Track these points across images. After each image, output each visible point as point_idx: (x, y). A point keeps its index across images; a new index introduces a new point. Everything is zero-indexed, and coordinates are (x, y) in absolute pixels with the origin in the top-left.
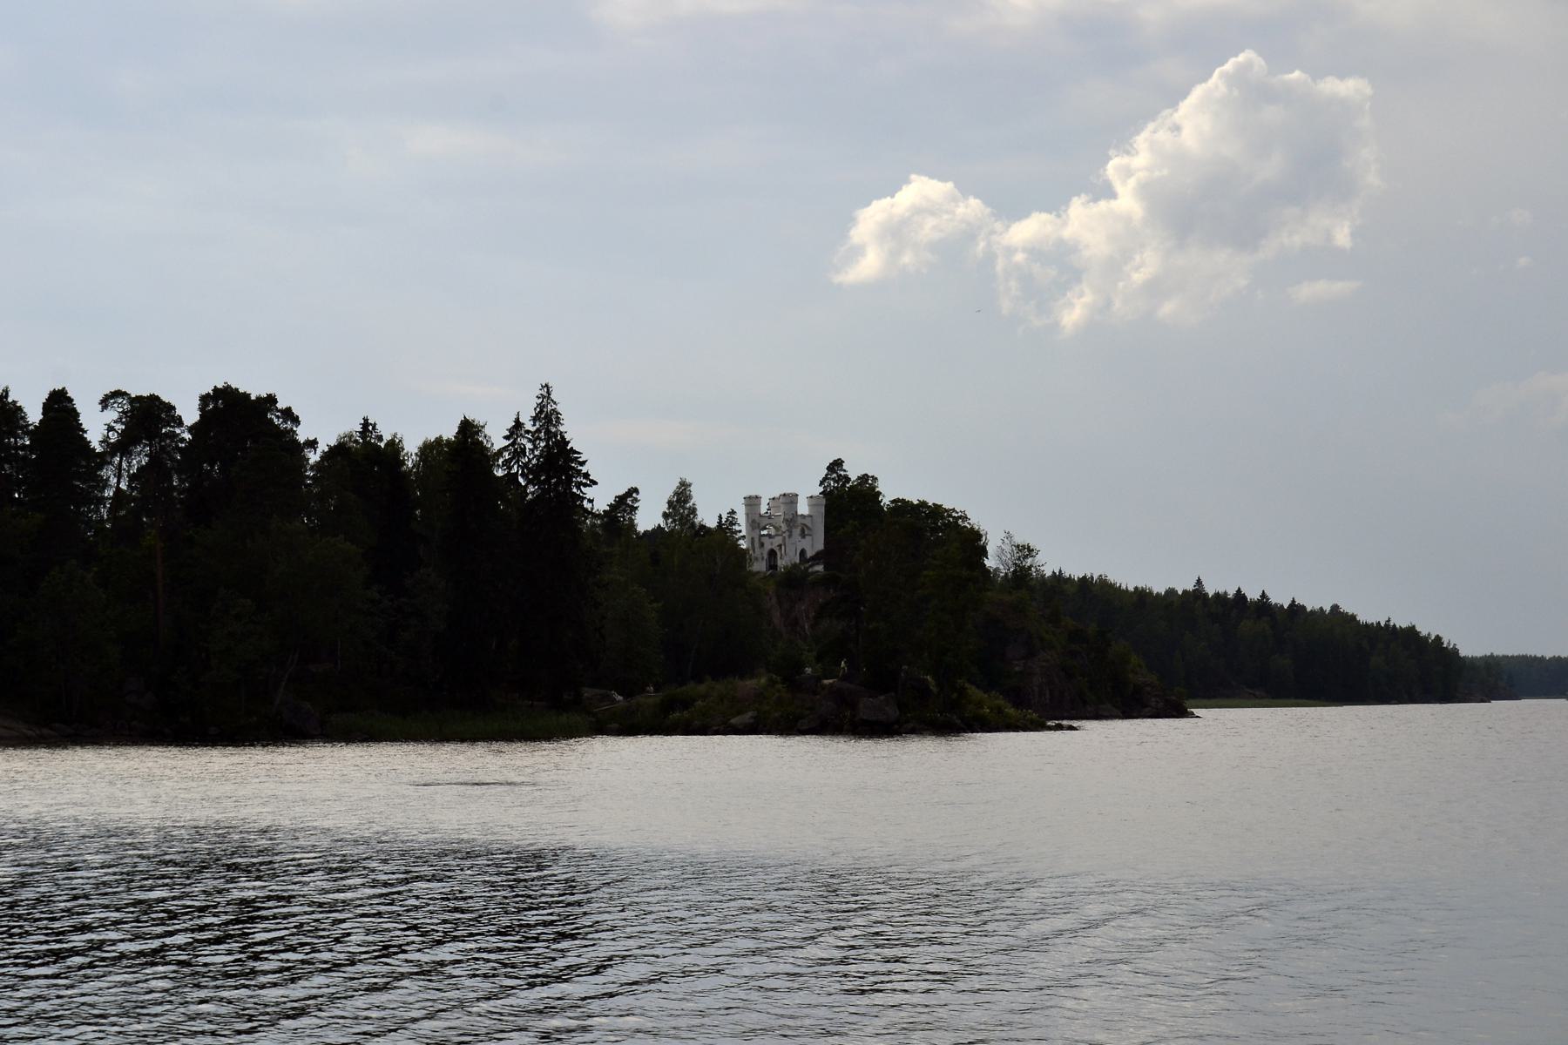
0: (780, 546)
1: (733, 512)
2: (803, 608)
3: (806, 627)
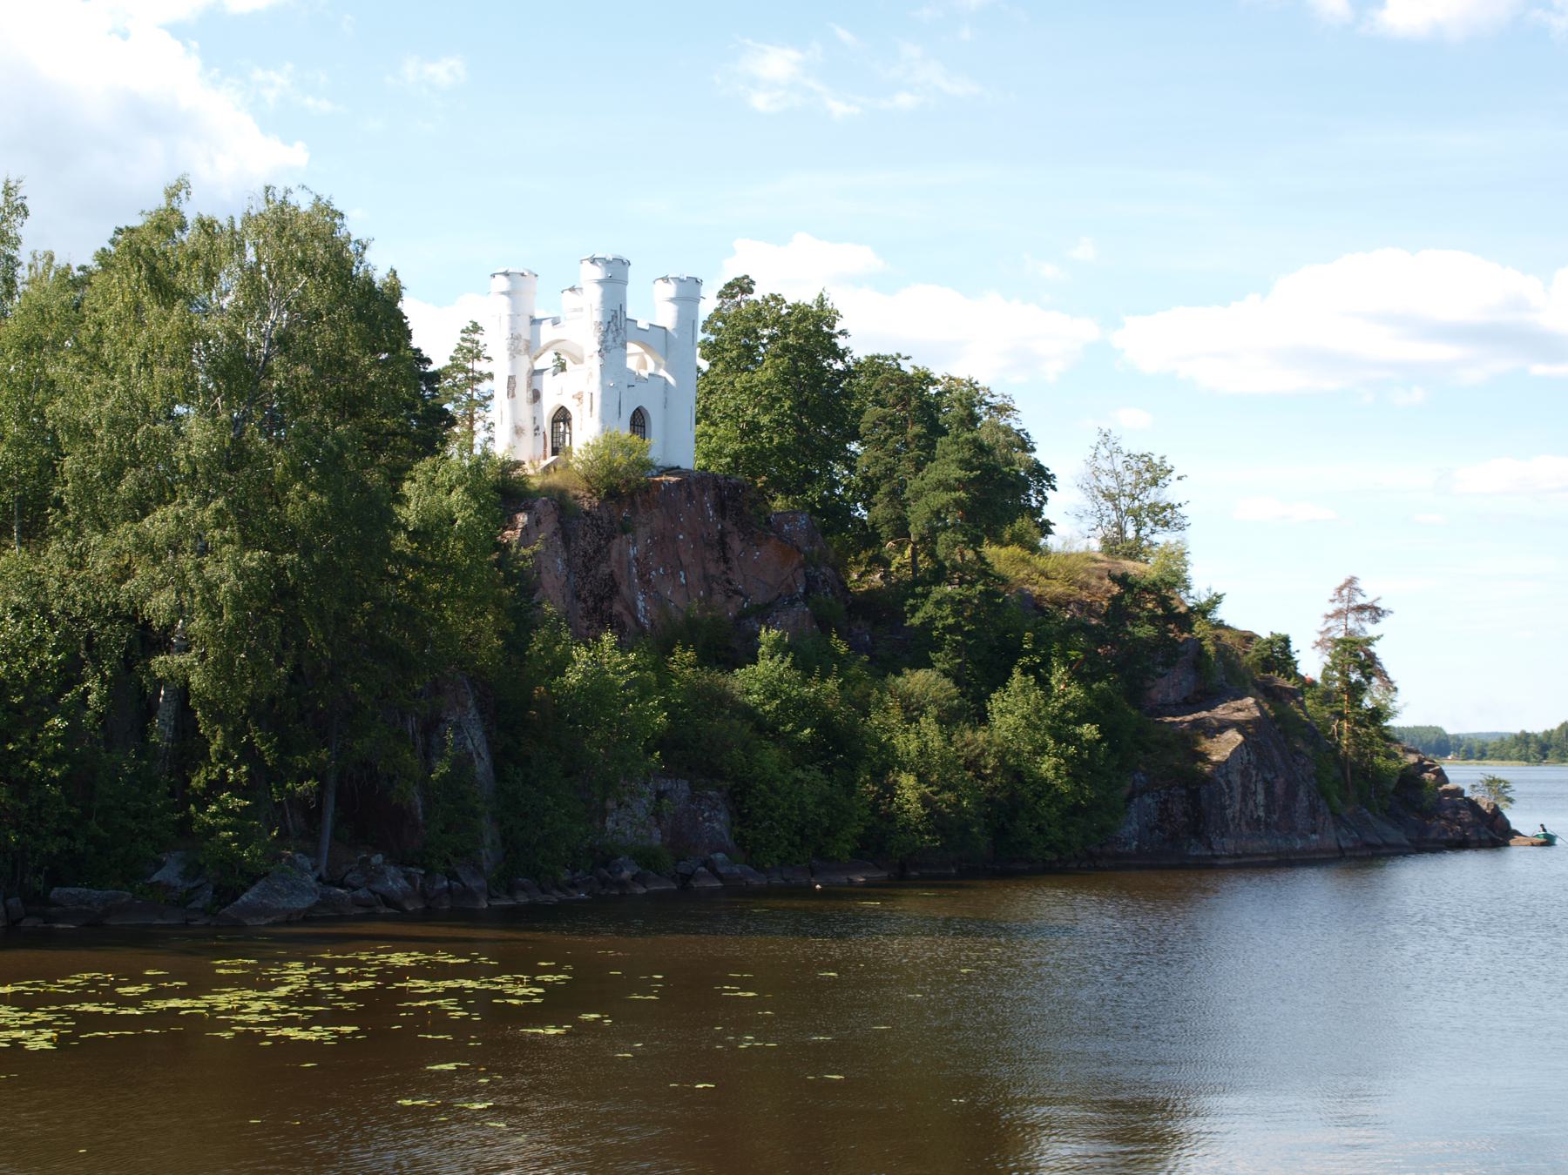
0: (579, 397)
1: (476, 328)
2: (632, 552)
3: (640, 604)
